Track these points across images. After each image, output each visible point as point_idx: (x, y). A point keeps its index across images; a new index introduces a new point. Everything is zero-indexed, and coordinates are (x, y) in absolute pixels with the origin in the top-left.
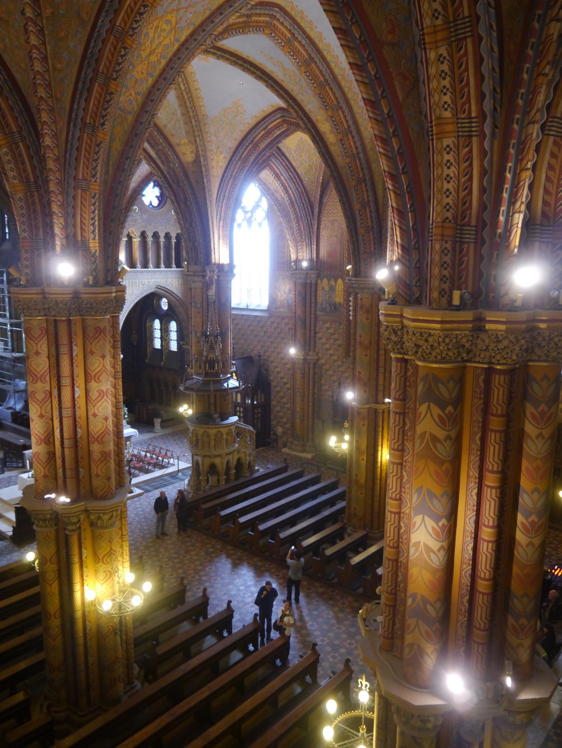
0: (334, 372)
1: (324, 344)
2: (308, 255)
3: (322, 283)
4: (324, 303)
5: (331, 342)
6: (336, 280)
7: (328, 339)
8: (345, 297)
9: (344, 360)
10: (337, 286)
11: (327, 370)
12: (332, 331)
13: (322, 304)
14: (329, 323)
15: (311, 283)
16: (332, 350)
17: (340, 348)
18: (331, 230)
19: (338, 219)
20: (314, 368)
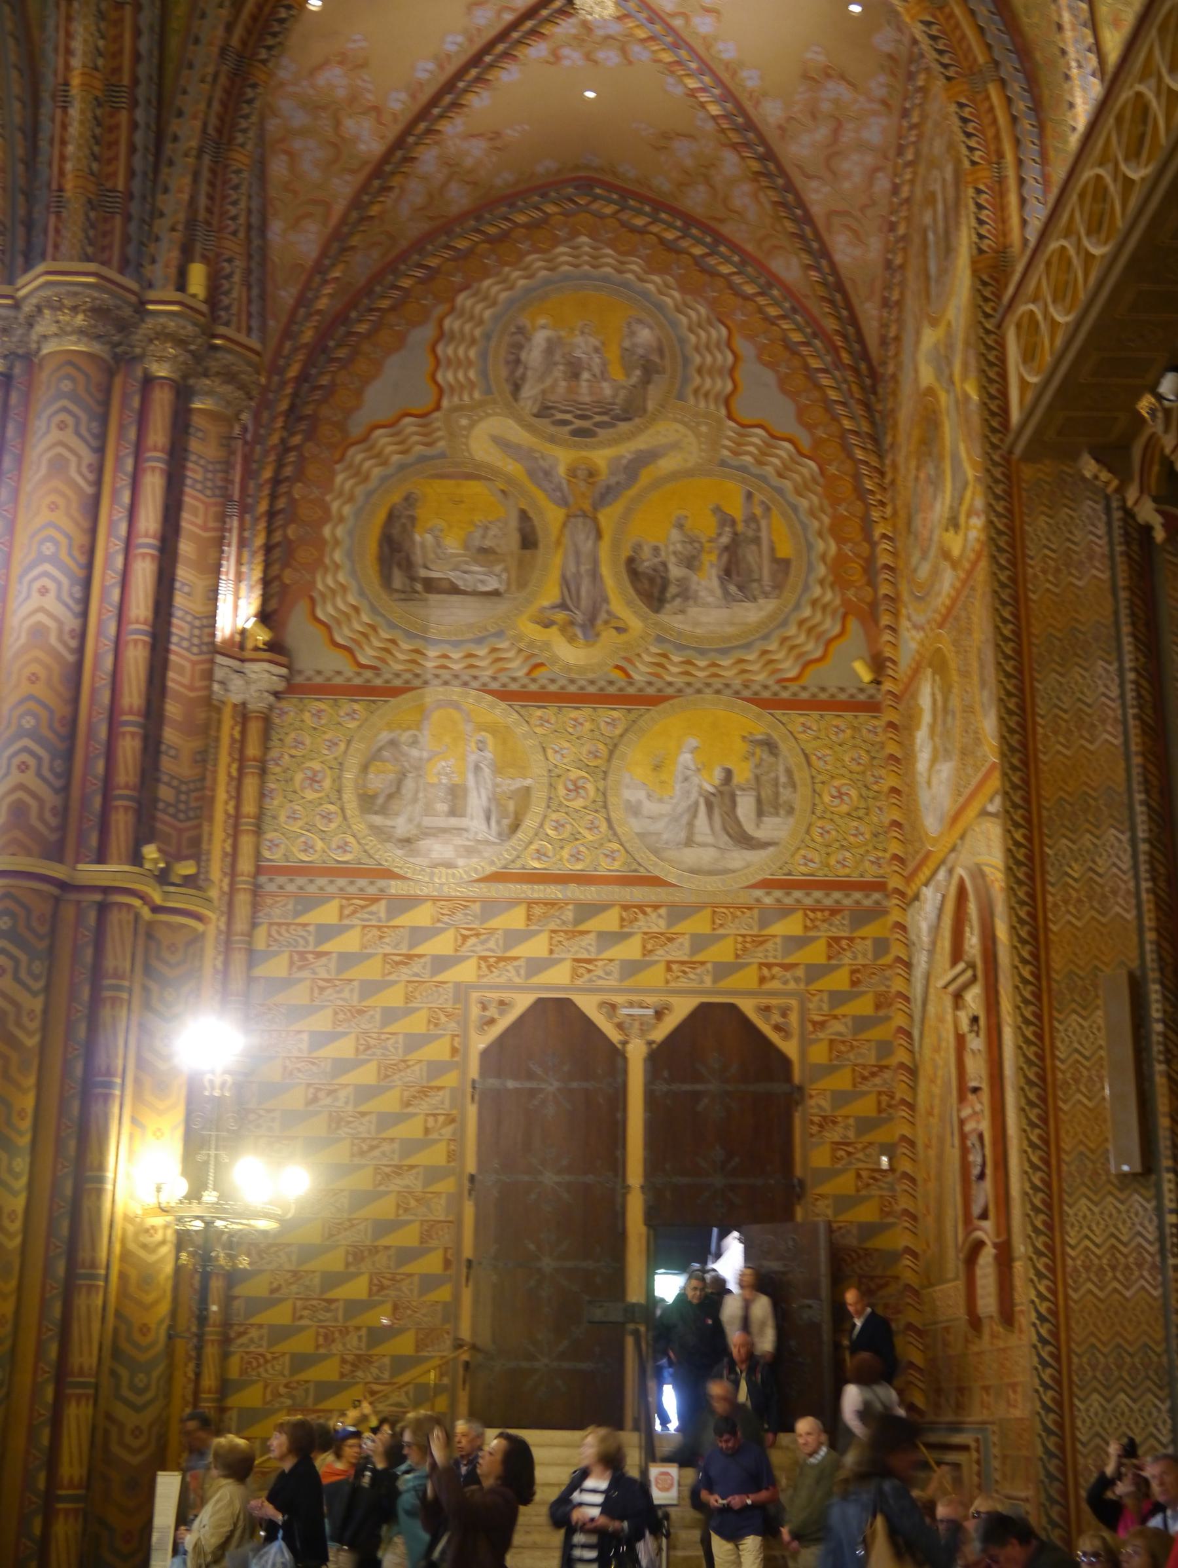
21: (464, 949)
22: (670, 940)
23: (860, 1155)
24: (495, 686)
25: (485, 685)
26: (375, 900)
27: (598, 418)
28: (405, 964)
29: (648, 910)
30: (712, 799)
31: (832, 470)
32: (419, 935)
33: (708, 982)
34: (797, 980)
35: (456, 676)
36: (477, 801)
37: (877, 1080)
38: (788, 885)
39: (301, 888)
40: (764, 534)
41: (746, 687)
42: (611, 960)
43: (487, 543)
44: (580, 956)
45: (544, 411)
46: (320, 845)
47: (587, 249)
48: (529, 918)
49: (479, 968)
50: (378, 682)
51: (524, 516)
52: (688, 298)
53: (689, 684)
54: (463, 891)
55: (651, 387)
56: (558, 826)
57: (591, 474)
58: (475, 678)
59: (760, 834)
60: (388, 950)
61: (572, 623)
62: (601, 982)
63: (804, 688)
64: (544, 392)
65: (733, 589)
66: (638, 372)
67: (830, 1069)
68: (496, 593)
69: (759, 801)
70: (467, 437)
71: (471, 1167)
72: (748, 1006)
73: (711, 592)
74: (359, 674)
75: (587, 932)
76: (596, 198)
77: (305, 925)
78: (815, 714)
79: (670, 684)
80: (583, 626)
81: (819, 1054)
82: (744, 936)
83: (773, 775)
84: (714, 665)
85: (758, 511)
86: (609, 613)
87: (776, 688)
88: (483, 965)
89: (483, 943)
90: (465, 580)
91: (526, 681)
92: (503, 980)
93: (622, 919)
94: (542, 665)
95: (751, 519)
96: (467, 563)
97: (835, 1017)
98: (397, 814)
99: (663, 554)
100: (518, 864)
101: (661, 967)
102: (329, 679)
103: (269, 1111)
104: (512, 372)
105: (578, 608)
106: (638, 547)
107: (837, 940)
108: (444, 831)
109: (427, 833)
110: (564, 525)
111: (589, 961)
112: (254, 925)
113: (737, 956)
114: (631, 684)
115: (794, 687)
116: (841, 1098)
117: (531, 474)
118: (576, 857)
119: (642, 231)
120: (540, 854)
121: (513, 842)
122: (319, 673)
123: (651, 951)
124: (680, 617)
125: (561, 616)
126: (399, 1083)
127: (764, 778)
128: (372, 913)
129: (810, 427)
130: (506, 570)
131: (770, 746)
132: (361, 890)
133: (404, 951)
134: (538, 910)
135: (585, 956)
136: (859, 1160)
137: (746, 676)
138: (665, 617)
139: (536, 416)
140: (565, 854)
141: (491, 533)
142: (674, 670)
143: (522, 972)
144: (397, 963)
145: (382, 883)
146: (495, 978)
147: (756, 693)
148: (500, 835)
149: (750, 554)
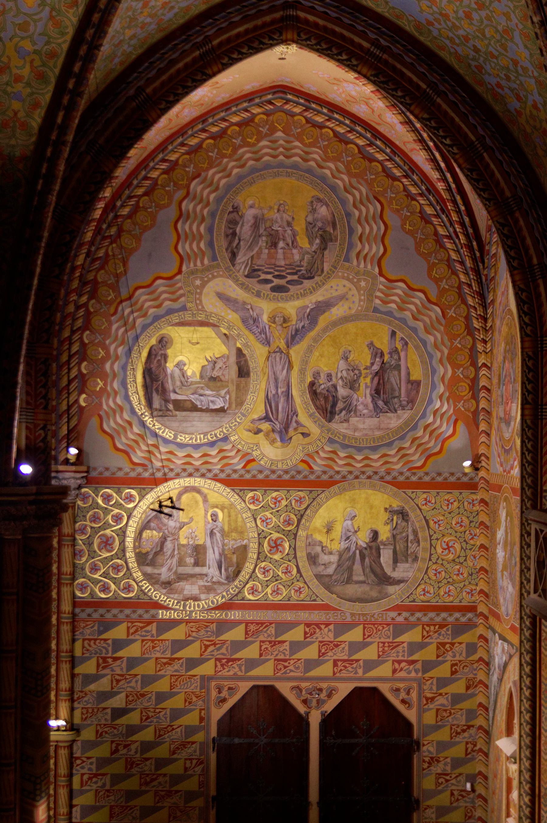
0: (130, 763)
21: (206, 653)
22: (337, 646)
23: (454, 781)
24: (222, 476)
25: (216, 475)
26: (149, 623)
27: (290, 278)
28: (170, 664)
29: (323, 627)
30: (364, 551)
31: (451, 313)
32: (178, 645)
33: (360, 672)
34: (417, 671)
35: (197, 470)
36: (212, 556)
37: (466, 734)
38: (412, 609)
39: (102, 616)
40: (402, 363)
41: (389, 473)
42: (299, 660)
43: (215, 374)
44: (279, 657)
45: (252, 273)
46: (113, 587)
47: (281, 142)
48: (246, 633)
49: (216, 666)
50: (146, 475)
51: (239, 352)
52: (354, 181)
53: (350, 472)
54: (205, 616)
55: (326, 252)
56: (265, 571)
57: (285, 320)
58: (210, 471)
59: (396, 575)
60: (158, 655)
61: (273, 431)
62: (292, 674)
63: (427, 474)
64: (252, 257)
65: (380, 403)
66: (318, 241)
67: (436, 728)
68: (222, 410)
69: (395, 552)
70: (200, 294)
71: (213, 792)
72: (385, 689)
73: (366, 406)
74: (133, 470)
75: (284, 642)
76: (288, 101)
77: (105, 640)
78: (434, 492)
79: (338, 472)
80: (280, 432)
81: (429, 718)
82: (384, 643)
83: (404, 534)
84: (367, 458)
85: (399, 346)
86: (297, 422)
87: (408, 474)
88: (218, 664)
89: (218, 649)
90: (201, 401)
91: (243, 472)
92: (231, 673)
93: (306, 633)
94: (253, 460)
95: (394, 351)
96: (202, 388)
97: (441, 694)
98: (162, 566)
99: (334, 379)
100: (240, 597)
101: (331, 663)
102: (114, 474)
103: (89, 758)
104: (230, 243)
105: (277, 419)
106: (317, 375)
107: (443, 644)
108: (193, 576)
109: (181, 577)
110: (268, 358)
111: (285, 660)
112: (74, 641)
113: (379, 656)
114: (312, 473)
115: (420, 473)
116: (442, 746)
117: (244, 321)
118: (276, 592)
119: (321, 127)
120: (253, 590)
121: (236, 583)
122: (107, 469)
123: (324, 654)
124: (345, 425)
125: (265, 426)
126: (168, 739)
127: (398, 537)
128: (147, 632)
129: (437, 281)
130: (228, 392)
131: (403, 514)
132: (140, 616)
133: (169, 656)
134: (252, 627)
135: (282, 657)
136: (453, 784)
137: (388, 466)
138: (334, 425)
139: (247, 276)
140: (269, 590)
141: (218, 366)
142: (341, 462)
143: (243, 668)
144: (165, 664)
145: (153, 612)
146: (225, 673)
147: (395, 478)
148: (227, 578)
149: (393, 378)
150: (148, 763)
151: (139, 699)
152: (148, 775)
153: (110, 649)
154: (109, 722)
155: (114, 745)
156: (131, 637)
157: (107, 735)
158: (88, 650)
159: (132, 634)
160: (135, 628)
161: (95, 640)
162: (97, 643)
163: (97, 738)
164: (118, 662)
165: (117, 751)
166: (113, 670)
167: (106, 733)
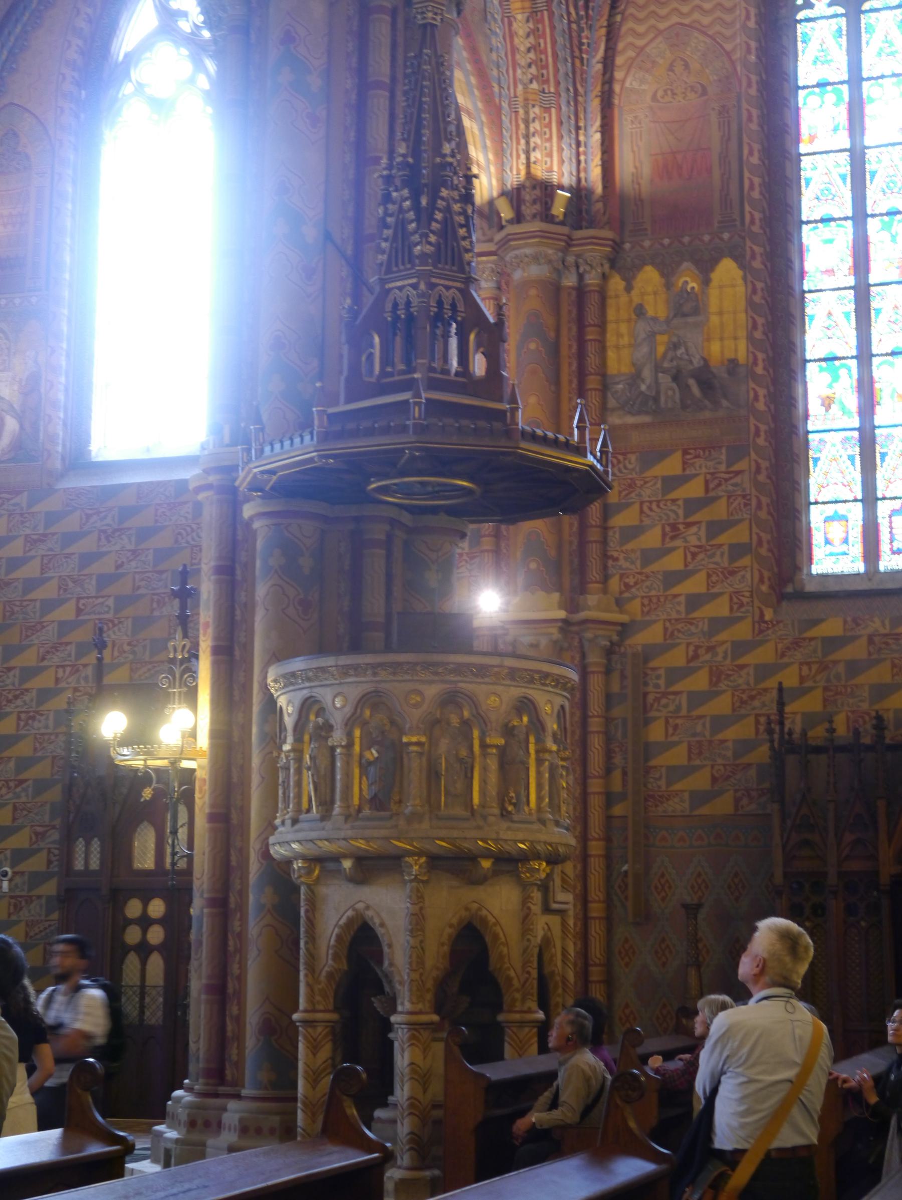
0: (716, 675)
1: (649, 556)
2: (566, 169)
3: (629, 289)
4: (647, 373)
5: (693, 541)
6: (706, 267)
7: (673, 531)
8: (758, 335)
9: (768, 615)
10: (713, 292)
11: (675, 675)
12: (694, 489)
13: (636, 377)
14: (678, 454)
15: (581, 291)
16: (701, 577)
17: (746, 561)
18: (671, 68)
19: (706, 20)
20: (608, 671)
150: (743, 673)
151: (727, 578)
152: (744, 691)
153: (681, 512)
154: (683, 616)
155: (691, 648)
156: (711, 494)
157: (680, 635)
158: (648, 516)
159: (714, 489)
160: (716, 482)
161: (658, 502)
162: (661, 505)
163: (665, 640)
164: (694, 529)
165: (696, 656)
166: (686, 541)
167: (679, 631)
